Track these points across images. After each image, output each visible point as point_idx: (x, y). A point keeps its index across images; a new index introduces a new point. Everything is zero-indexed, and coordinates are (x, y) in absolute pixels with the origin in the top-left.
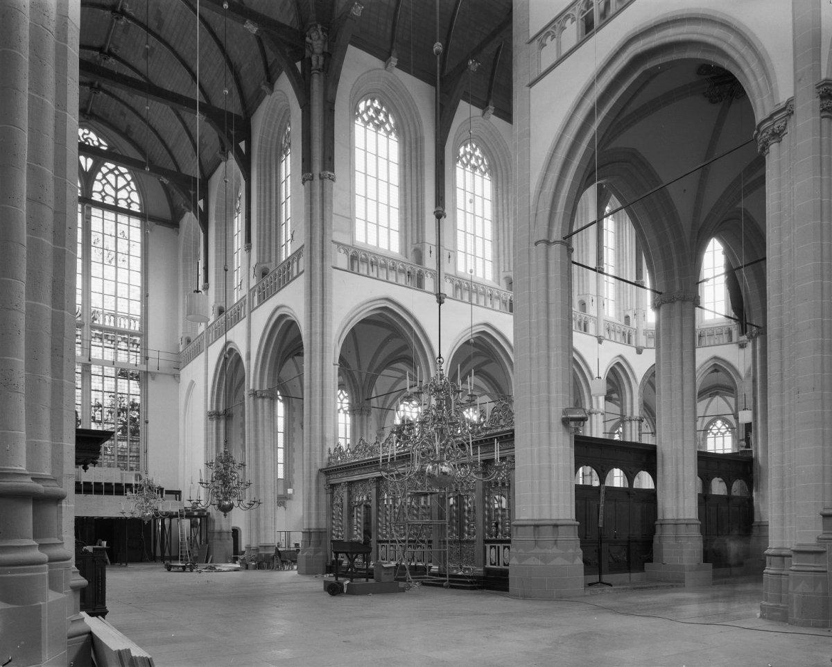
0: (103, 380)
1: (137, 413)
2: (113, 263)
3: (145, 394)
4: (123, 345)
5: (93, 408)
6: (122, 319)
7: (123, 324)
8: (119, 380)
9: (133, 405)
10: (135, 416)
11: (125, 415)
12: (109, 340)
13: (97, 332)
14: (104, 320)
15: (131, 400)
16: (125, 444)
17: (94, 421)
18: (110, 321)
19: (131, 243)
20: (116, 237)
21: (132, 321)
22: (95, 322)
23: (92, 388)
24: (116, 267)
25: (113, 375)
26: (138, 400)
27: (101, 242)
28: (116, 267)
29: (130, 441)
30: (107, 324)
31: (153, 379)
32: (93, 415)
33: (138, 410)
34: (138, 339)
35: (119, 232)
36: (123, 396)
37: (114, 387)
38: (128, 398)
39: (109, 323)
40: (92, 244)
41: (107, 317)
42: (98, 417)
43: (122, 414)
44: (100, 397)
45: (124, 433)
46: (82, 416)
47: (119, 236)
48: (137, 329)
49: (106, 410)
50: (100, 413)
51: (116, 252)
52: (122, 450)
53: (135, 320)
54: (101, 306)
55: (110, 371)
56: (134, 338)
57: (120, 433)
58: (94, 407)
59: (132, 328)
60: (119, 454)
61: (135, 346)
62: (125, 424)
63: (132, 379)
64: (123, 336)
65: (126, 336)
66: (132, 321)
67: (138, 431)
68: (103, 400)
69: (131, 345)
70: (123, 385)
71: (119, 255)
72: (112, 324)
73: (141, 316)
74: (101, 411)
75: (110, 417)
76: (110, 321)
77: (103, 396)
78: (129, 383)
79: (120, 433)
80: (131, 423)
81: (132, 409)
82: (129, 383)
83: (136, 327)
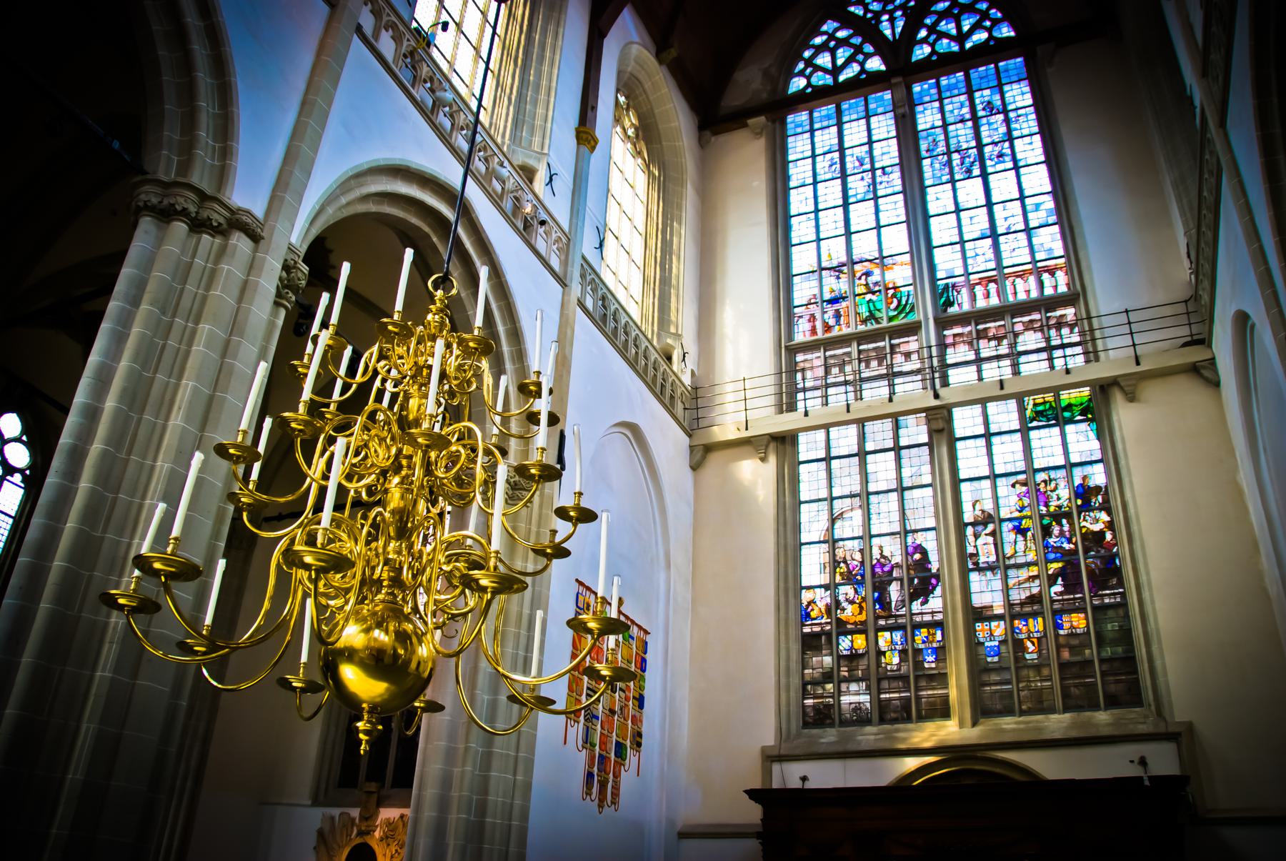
0: (989, 446)
1: (1104, 517)
2: (976, 172)
3: (1110, 456)
4: (1031, 340)
5: (970, 530)
6: (1018, 281)
7: (1025, 290)
8: (1033, 434)
9: (1084, 493)
10: (1097, 527)
11: (1066, 528)
12: (990, 340)
13: (957, 330)
14: (973, 298)
15: (1077, 481)
16: (1078, 621)
17: (978, 569)
18: (987, 296)
19: (1012, 115)
20: (975, 119)
21: (1045, 276)
22: (953, 310)
23: (962, 475)
24: (984, 176)
25: (1016, 425)
26: (1098, 476)
27: (943, 143)
28: (984, 176)
29: (1095, 608)
30: (981, 303)
31: (1131, 398)
32: (970, 550)
33: (1105, 507)
34: (1069, 312)
35: (979, 107)
36: (1053, 474)
37: (1020, 456)
38: (1070, 478)
39: (987, 300)
40: (924, 154)
41: (979, 291)
42: (987, 554)
43: (1056, 530)
44: (987, 493)
45: (1072, 585)
46: (940, 561)
47: (981, 114)
48: (1063, 289)
49: (1007, 526)
50: (990, 539)
51: (980, 146)
52: (1075, 642)
53: (1052, 272)
54: (960, 271)
55: (1005, 415)
56: (1058, 313)
57: (1058, 588)
58: (973, 524)
59: (1048, 291)
60: (1066, 655)
61: (1065, 331)
62: (1069, 559)
63: (1071, 421)
64: (1026, 319)
65: (1036, 316)
66: (1045, 276)
67: (1117, 572)
68: (996, 498)
69: (1053, 332)
70: (1047, 445)
71: (987, 150)
72: (994, 301)
73: (1067, 255)
74: (993, 534)
75: (1021, 545)
76: (987, 296)
77: (994, 487)
78: (1063, 435)
79: (1058, 588)
80: (1086, 551)
81: (1086, 507)
82: (1063, 435)
83: (1059, 283)
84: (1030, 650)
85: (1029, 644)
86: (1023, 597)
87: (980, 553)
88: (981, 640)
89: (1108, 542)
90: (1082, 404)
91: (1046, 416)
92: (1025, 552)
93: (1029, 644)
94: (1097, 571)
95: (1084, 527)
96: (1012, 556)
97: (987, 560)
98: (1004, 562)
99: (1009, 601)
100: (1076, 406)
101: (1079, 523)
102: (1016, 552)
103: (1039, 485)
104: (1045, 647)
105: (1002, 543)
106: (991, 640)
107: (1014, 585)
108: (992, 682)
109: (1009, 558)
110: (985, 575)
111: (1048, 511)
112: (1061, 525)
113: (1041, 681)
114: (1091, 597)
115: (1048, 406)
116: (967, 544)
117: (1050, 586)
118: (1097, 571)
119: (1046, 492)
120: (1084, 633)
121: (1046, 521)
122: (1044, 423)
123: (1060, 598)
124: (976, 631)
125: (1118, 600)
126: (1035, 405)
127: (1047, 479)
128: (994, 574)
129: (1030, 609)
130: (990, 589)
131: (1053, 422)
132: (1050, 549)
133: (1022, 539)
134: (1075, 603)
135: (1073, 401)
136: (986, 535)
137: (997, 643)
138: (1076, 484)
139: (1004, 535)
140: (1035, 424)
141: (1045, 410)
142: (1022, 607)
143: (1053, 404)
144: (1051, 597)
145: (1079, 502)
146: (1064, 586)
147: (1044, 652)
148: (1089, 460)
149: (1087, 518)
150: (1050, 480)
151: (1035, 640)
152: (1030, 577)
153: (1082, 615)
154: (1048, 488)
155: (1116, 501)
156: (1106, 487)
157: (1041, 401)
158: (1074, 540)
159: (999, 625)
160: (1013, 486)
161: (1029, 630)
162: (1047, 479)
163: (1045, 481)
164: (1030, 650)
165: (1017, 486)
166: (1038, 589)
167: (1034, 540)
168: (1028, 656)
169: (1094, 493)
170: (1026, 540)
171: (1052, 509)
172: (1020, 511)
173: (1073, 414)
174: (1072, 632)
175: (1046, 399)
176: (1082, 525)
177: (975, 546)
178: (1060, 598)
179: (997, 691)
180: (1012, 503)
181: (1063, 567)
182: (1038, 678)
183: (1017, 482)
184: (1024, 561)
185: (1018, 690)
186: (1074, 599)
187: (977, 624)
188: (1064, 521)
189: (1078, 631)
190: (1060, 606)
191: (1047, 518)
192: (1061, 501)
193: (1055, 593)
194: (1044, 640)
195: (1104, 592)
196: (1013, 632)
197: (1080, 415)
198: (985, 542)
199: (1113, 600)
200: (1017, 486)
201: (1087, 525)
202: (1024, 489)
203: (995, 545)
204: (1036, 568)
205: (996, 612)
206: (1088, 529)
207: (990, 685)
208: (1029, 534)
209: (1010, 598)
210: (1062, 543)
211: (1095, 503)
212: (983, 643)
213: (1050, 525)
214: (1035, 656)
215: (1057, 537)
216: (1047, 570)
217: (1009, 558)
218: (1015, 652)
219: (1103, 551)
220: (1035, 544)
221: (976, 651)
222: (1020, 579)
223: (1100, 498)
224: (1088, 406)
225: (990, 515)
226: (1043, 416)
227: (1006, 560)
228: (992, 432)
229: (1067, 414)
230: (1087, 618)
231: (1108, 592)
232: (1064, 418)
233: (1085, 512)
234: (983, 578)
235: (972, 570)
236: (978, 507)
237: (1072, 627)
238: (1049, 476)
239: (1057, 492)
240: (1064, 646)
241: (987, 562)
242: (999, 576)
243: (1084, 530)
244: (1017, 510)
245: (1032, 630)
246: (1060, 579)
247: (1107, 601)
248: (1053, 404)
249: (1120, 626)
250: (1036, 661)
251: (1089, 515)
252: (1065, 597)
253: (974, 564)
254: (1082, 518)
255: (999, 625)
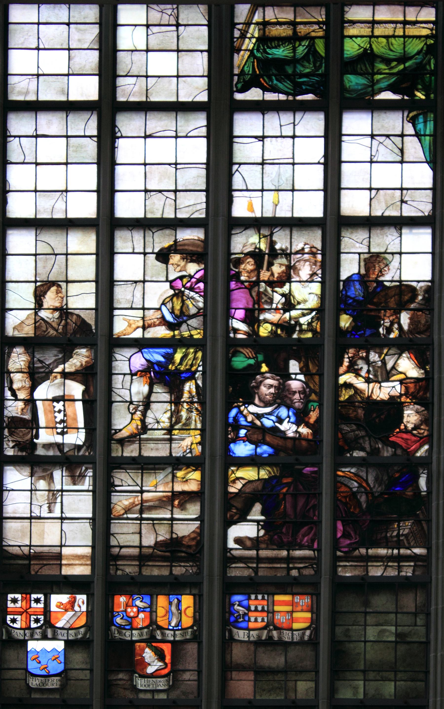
92: (170, 430)
95: (348, 386)
97: (59, 439)
98: (109, 450)
99: (108, 546)
102: (144, 428)
107: (128, 510)
109: (122, 442)
123: (253, 553)
129: (165, 572)
133: (166, 397)
134: (289, 569)
139: (117, 381)
144: (225, 549)
149: (361, 364)
152: (175, 495)
158: (313, 416)
166: (194, 526)
167: (202, 403)
176: (342, 380)
178: (253, 553)
186: (289, 559)
190: (246, 573)
191: (247, 351)
193: (238, 541)
204: (196, 475)
206: (357, 391)
209: (113, 542)
210: (280, 421)
215: (267, 404)
216: (226, 482)
220: (202, 414)
222: (146, 496)
233: (359, 347)
234: (42, 484)
241: (60, 446)
242: (87, 484)
243: (345, 395)
246: (258, 507)
253: (18, 445)
254: (346, 362)
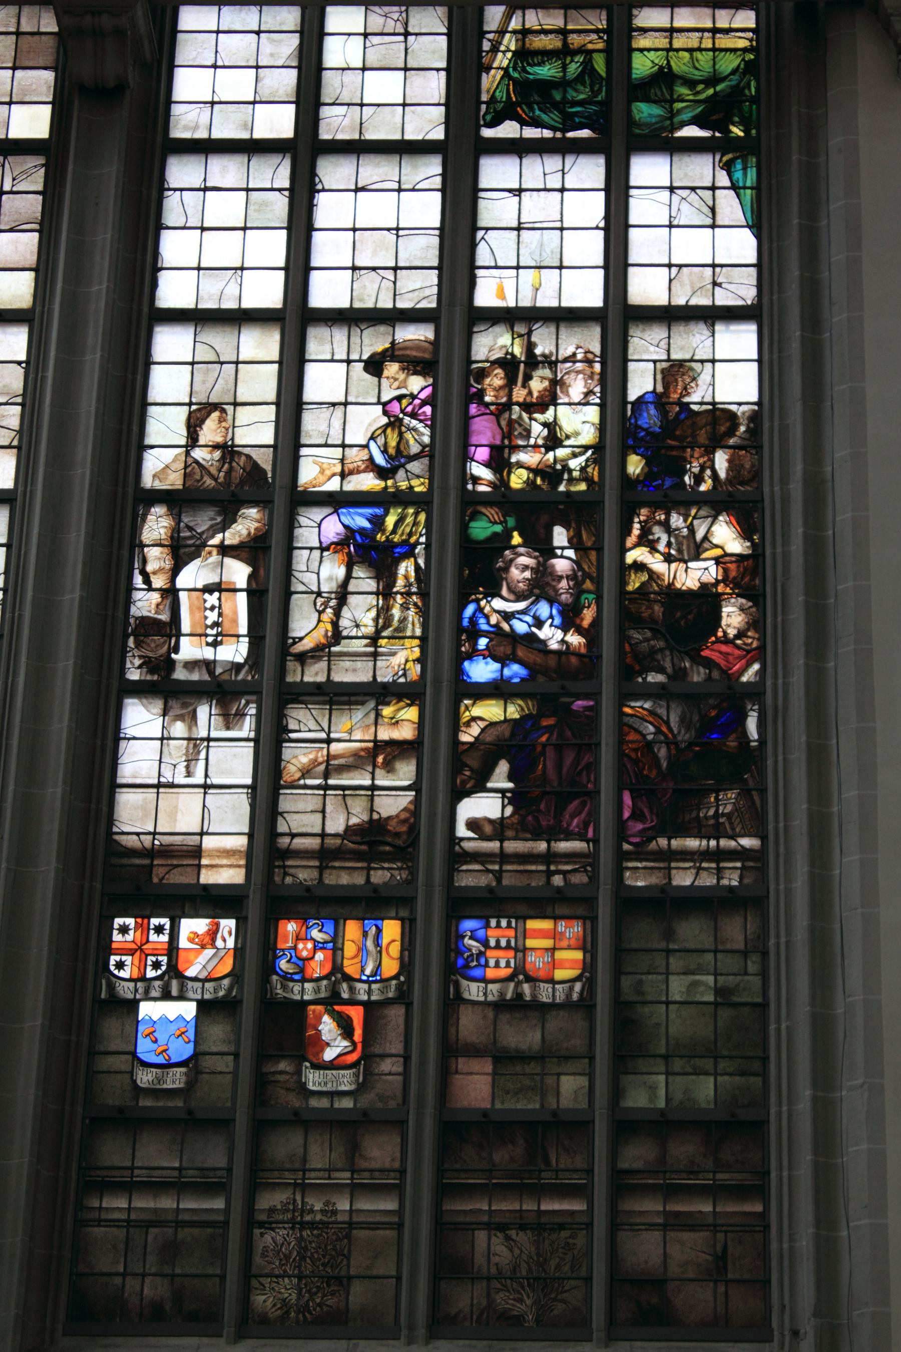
84: (329, 1055)
85: (328, 1027)
86: (336, 824)
87: (186, 625)
88: (126, 991)
89: (726, 640)
90: (713, 80)
91: (559, 107)
92: (374, 639)
93: (328, 1027)
94: (662, 753)
95: (639, 567)
96: (320, 651)
97: (208, 653)
98: (282, 671)
99: (273, 834)
100: (691, 83)
101: (623, 550)
102: (337, 636)
103: (482, 374)
104: (397, 1047)
105: (288, 594)
106: (166, 996)
107: (306, 772)
108: (140, 1176)
109: (302, 658)
110: (193, 718)
111: (501, 484)
112: (547, 551)
113: (355, 1189)
114: (622, 856)
115: (573, 68)
116: (138, 580)
117: (460, 794)
118: (662, 753)
119: (507, 406)
120: (567, 1005)
121: (481, 529)
122: (547, 134)
123: (494, 845)
124: (107, 948)
125: (732, 879)
126: (523, 55)
127: (518, 351)
128: (230, 719)
129: (359, 879)
130: (199, 779)
131: (585, 133)
132: (483, 642)
133: (371, 585)
134: (549, 874)
135: (680, 64)
136: (225, 550)
137: (188, 1010)
138: (633, 394)
139: (301, 559)
140: (508, 130)
141: (563, 84)
142: (321, 869)
143: (600, 65)
144: (453, 839)
145: (635, 465)
146: (514, 798)
147: (387, 1066)
148: (703, 300)
149: (658, 532)
150: (532, 362)
151: (356, 1014)
152: (379, 746)
153: (572, 930)
154: (519, 394)
155: (785, 480)
156: (754, 418)
157: (550, 42)
158: (588, 615)
159: (213, 933)
160: (374, 366)
161: (337, 968)
162: (518, 351)
163: (508, 364)
164: (329, 1055)
165: (392, 369)
166: (405, 799)
167: (423, 594)
168: (313, 1079)
169: (703, 437)
170: (386, 593)
171: (518, 480)
172: (382, 473)
173: (672, 114)
174: (519, 996)
175: (575, 40)
176: (631, 557)
177: (171, 593)
178: (494, 845)
179: (156, 1220)
180: (356, 436)
181: (523, 718)
182: (344, 1177)
183: (392, 353)
184: (364, 677)
185: (251, 1222)
186: (550, 857)
187: (118, 921)
188: (560, 537)
189: (545, 993)
190: (484, 880)
191: (492, 512)
192: (561, 453)
193: (472, 824)
194: (396, 1014)
195: (675, 843)
196: (268, 967)
197: (697, 121)
198: (213, 578)
199: (707, 880)
200: (392, 369)
201: (657, 564)
202: (416, 384)
203: (256, 594)
204: (411, 714)
205: (207, 877)
206: (653, 576)
207: (129, 1187)
208: (406, 568)
209: (282, 827)
210: (539, 624)
211: (699, 479)
212: (132, 1006)
213: (500, 542)
214: (345, 1081)
215: (519, 597)
216: (456, 726)
217: (302, 658)
218: (262, 1056)
219: (698, 675)
220: (423, 612)
221: (94, 1035)
222: (335, 747)
223: (721, 460)
224: (737, 91)
225: (255, 468)
226: (548, 104)
227: (292, 665)
228: (325, 135)
229: (645, 111)
230: (588, 946)
231: (693, 843)
232: (631, 122)
233: (655, 506)
234: (179, 729)
235: (141, 690)
236: (210, 432)
237: (520, 973)
238: (530, 347)
239: (549, 415)
240: (474, 1051)
241: (209, 665)
242: (247, 728)
243: (635, 582)
244: (371, 465)
245: (351, 969)
246: (503, 767)
247: (683, 879)
248: (600, 65)
249: (719, 991)
250: (347, 1103)
251: (666, 525)
252: (512, 846)
253: (148, 664)
254: (636, 530)
255: (213, 933)
